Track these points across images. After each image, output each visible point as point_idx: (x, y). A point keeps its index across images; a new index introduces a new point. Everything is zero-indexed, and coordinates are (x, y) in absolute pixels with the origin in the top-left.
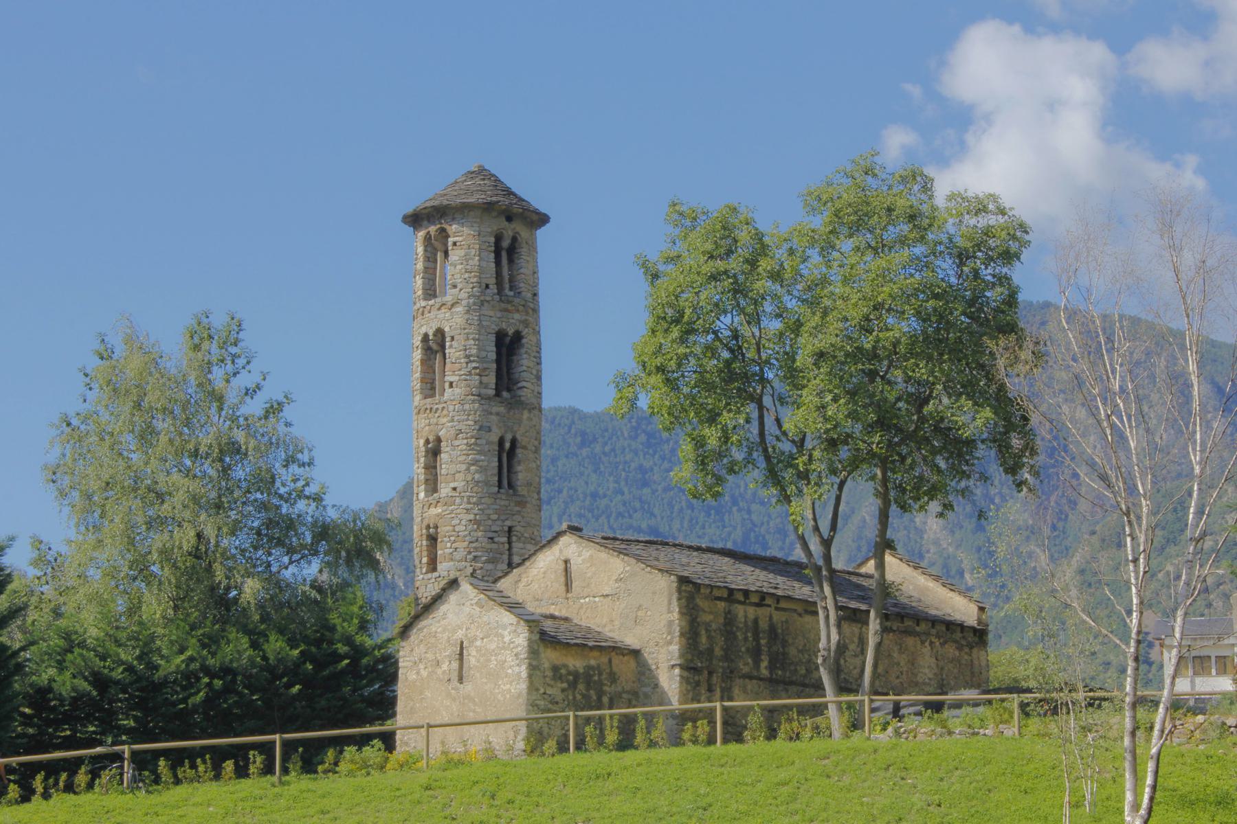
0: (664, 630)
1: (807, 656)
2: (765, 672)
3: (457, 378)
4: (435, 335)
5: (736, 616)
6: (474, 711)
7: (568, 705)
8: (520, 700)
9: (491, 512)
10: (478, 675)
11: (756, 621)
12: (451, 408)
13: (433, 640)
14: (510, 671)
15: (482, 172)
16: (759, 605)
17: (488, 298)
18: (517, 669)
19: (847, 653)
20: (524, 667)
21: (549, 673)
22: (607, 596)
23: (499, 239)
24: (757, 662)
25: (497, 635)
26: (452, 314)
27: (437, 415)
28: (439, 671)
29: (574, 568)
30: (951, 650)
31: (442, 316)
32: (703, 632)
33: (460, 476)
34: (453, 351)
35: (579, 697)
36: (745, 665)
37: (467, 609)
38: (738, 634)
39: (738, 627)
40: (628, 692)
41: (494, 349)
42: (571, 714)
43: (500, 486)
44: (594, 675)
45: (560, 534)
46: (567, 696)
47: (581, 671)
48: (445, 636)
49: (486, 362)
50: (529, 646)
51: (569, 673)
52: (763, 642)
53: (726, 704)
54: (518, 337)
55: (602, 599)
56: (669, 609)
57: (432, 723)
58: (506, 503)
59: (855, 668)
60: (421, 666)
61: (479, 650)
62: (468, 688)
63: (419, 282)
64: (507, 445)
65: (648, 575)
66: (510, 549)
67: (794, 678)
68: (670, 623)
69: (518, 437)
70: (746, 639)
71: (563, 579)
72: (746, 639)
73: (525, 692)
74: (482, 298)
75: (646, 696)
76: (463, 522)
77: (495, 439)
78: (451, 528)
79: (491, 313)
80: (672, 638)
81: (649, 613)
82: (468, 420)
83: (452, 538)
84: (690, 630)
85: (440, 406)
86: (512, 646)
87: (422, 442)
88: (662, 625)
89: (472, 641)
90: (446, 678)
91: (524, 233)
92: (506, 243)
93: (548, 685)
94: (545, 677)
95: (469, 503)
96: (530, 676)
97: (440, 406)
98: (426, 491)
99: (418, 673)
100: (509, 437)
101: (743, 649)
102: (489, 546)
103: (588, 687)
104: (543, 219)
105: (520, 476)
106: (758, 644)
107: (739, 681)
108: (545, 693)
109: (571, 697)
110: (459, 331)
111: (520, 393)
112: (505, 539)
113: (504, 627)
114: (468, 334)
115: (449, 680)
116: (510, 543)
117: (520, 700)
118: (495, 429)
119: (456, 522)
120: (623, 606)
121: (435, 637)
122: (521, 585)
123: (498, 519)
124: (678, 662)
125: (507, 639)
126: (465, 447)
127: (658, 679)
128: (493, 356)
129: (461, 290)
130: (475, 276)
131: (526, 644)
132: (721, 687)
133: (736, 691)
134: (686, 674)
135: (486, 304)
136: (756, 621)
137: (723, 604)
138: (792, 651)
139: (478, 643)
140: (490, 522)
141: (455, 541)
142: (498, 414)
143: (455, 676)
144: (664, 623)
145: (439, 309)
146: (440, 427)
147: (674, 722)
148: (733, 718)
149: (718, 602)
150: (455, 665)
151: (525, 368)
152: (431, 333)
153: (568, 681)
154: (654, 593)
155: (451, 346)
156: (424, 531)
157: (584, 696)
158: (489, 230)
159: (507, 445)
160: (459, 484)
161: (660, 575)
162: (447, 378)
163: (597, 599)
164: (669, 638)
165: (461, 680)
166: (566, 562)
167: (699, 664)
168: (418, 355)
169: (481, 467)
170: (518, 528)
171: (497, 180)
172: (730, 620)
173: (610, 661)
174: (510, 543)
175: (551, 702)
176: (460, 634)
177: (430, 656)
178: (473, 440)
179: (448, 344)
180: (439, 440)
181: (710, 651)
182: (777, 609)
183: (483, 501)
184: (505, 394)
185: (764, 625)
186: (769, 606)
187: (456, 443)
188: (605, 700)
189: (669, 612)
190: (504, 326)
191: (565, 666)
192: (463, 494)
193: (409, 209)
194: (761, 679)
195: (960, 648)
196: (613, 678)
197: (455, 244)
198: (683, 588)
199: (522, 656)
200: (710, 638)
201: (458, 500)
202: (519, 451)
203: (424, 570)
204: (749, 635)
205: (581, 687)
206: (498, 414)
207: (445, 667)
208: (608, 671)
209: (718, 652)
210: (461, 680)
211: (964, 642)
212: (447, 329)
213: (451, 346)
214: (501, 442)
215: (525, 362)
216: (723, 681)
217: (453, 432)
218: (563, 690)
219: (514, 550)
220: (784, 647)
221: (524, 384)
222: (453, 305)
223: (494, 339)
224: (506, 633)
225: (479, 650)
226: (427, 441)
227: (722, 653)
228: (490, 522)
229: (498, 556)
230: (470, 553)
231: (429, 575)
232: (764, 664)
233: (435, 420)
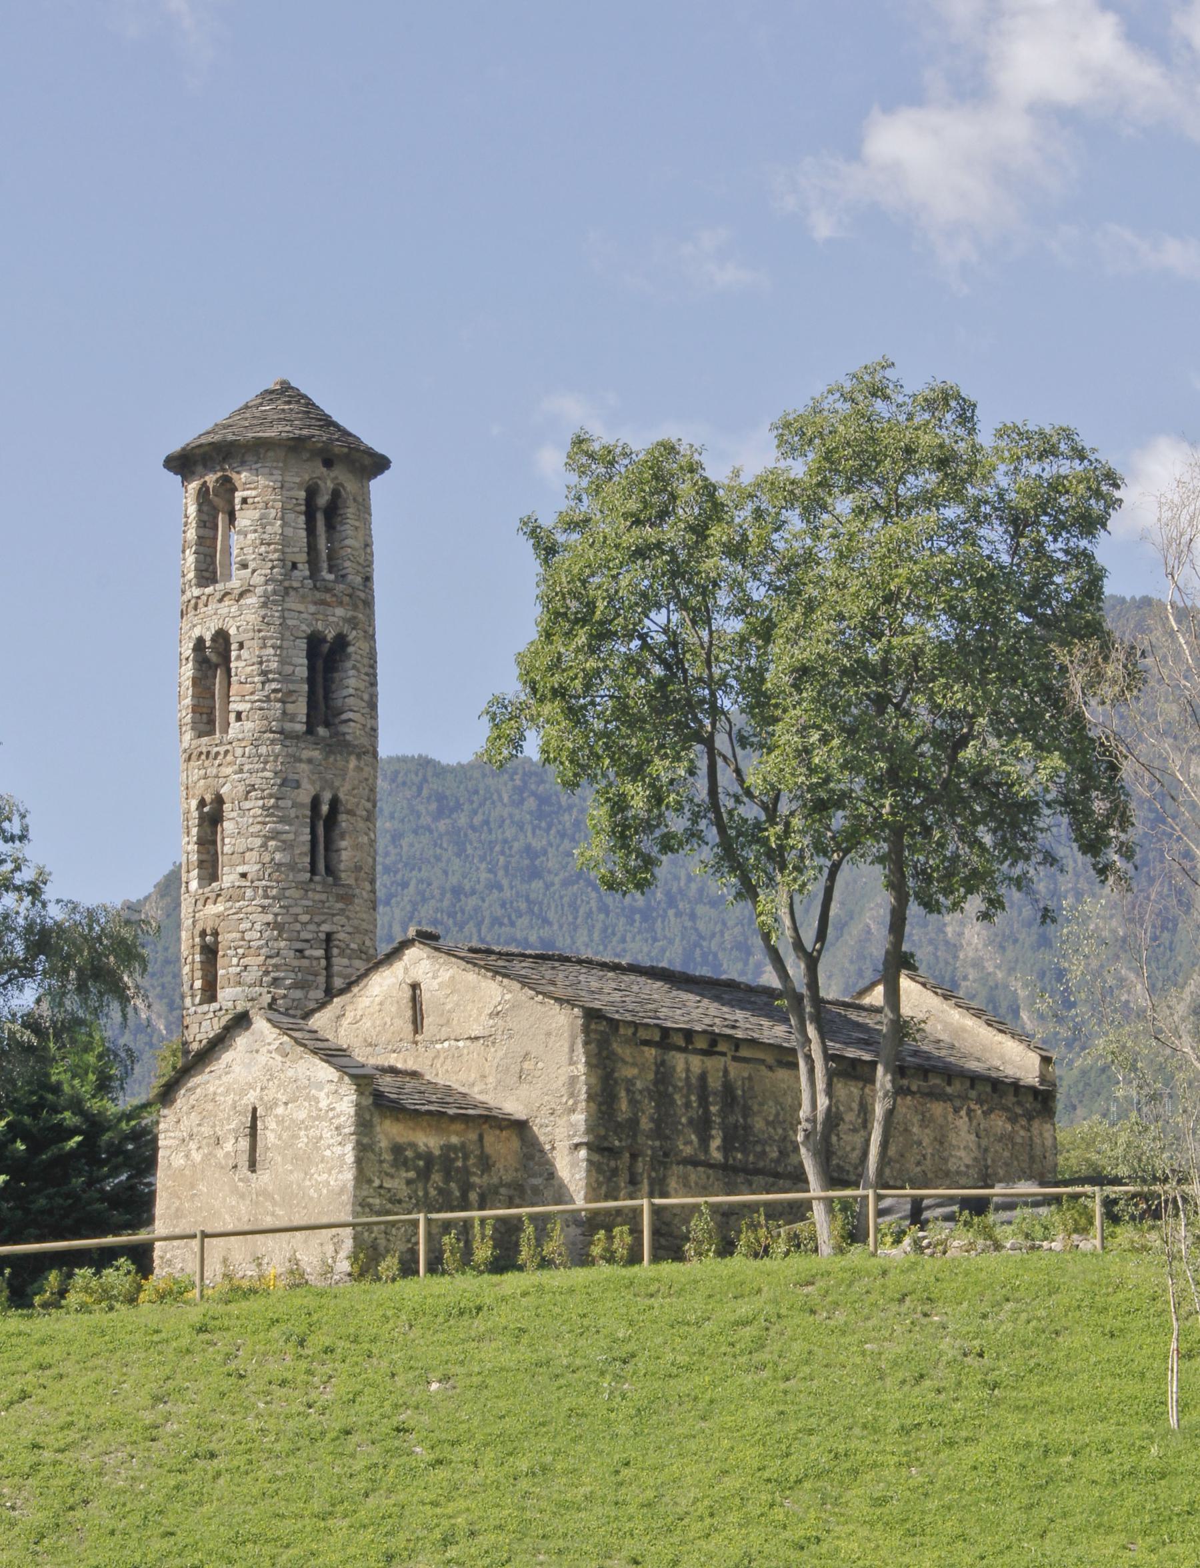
0: (563, 1091)
1: (780, 1131)
2: (717, 1155)
3: (248, 706)
4: (213, 640)
5: (674, 1068)
6: (273, 1214)
7: (417, 1205)
8: (344, 1198)
9: (299, 910)
10: (280, 1159)
11: (703, 1077)
12: (239, 752)
13: (210, 1106)
14: (328, 1153)
15: (285, 391)
16: (708, 1053)
17: (295, 584)
18: (338, 1150)
19: (843, 1127)
20: (349, 1147)
21: (388, 1157)
22: (477, 1038)
23: (312, 492)
24: (705, 1141)
25: (308, 1098)
27: (217, 762)
28: (220, 1154)
29: (426, 996)
30: (999, 1123)
31: (226, 610)
32: (623, 1094)
33: (252, 856)
34: (242, 665)
35: (433, 1192)
36: (687, 1145)
37: (262, 1059)
38: (677, 1096)
39: (675, 1087)
40: (508, 1186)
41: (305, 661)
42: (421, 1216)
43: (313, 871)
44: (457, 1159)
45: (405, 944)
46: (416, 1192)
47: (437, 1152)
48: (229, 1099)
49: (293, 682)
50: (357, 1114)
51: (419, 1156)
52: (713, 1109)
53: (657, 1201)
54: (341, 642)
55: (468, 1043)
56: (571, 1058)
57: (209, 1230)
58: (323, 897)
59: (853, 1149)
60: (193, 1145)
61: (280, 1121)
62: (263, 1178)
63: (191, 559)
64: (325, 808)
65: (539, 1007)
66: (328, 967)
67: (761, 1164)
68: (573, 1080)
69: (341, 796)
70: (688, 1105)
71: (409, 1013)
72: (688, 1105)
73: (351, 1184)
74: (286, 584)
75: (536, 1191)
76: (258, 927)
77: (307, 800)
78: (239, 935)
79: (301, 607)
80: (576, 1103)
81: (540, 1065)
82: (264, 770)
83: (240, 951)
84: (603, 1090)
85: (222, 749)
86: (331, 1114)
87: (194, 803)
88: (560, 1083)
89: (270, 1108)
90: (231, 1163)
91: (350, 486)
92: (323, 500)
93: (387, 1174)
94: (381, 1162)
95: (266, 897)
96: (359, 1161)
97: (222, 749)
98: (200, 878)
99: (187, 1156)
100: (327, 796)
101: (684, 1120)
102: (296, 963)
103: (448, 1178)
104: (380, 464)
105: (345, 855)
106: (707, 1112)
107: (677, 1170)
108: (381, 1187)
109: (421, 1194)
110: (251, 634)
111: (344, 728)
112: (320, 953)
113: (320, 1086)
114: (264, 638)
115: (235, 1167)
116: (328, 957)
117: (344, 1198)
118: (305, 784)
119: (245, 925)
120: (500, 1054)
121: (213, 1100)
122: (345, 1022)
123: (310, 922)
124: (585, 1140)
125: (323, 1104)
126: (259, 812)
127: (553, 1165)
128: (302, 672)
129: (254, 571)
130: (276, 551)
131: (352, 1111)
132: (649, 1177)
133: (673, 1184)
134: (596, 1157)
135: (292, 593)
136: (703, 1077)
137: (653, 1051)
138: (759, 1124)
139: (280, 1110)
140: (298, 927)
141: (244, 956)
142: (310, 761)
143: (244, 1160)
144: (563, 1079)
145: (221, 600)
146: (221, 780)
147: (579, 1231)
148: (667, 1224)
149: (646, 1049)
150: (244, 1144)
151: (351, 691)
152: (208, 637)
153: (416, 1168)
154: (548, 1034)
155: (239, 658)
156: (197, 940)
157: (441, 1191)
158: (297, 480)
159: (325, 808)
160: (252, 869)
161: (557, 1006)
162: (232, 706)
163: (461, 1044)
164: (571, 1102)
165: (253, 1166)
166: (415, 987)
167: (617, 1143)
168: (188, 670)
169: (284, 842)
170: (341, 936)
171: (310, 403)
172: (663, 1075)
173: (481, 1138)
174: (328, 957)
175: (390, 1201)
176: (252, 1097)
177: (206, 1130)
178: (272, 801)
179: (234, 654)
180: (219, 800)
181: (634, 1123)
183: (287, 893)
184: (322, 731)
185: (714, 1083)
186: (724, 1054)
187: (247, 805)
188: (473, 1196)
189: (572, 1063)
190: (320, 626)
191: (413, 1145)
192: (256, 883)
193: (175, 447)
195: (1013, 1119)
196: (486, 1164)
197: (244, 501)
198: (593, 1026)
199: (347, 1130)
200: (633, 1102)
201: (249, 893)
202: (342, 817)
203: (197, 1000)
204: (693, 1098)
205: (437, 1177)
206: (310, 761)
207: (229, 1146)
208: (478, 1152)
209: (645, 1124)
210: (253, 1166)
211: (1019, 1111)
212: (232, 631)
213: (239, 658)
214: (315, 803)
215: (352, 682)
216: (653, 1169)
217: (241, 788)
218: (409, 1182)
219: (336, 969)
221: (350, 715)
222: (241, 595)
223: (305, 646)
224: (322, 1095)
225: (280, 1121)
226: (202, 803)
227: (651, 1125)
228: (298, 927)
229: (311, 978)
230: (267, 973)
231: (205, 1007)
232: (716, 1143)
233: (214, 771)
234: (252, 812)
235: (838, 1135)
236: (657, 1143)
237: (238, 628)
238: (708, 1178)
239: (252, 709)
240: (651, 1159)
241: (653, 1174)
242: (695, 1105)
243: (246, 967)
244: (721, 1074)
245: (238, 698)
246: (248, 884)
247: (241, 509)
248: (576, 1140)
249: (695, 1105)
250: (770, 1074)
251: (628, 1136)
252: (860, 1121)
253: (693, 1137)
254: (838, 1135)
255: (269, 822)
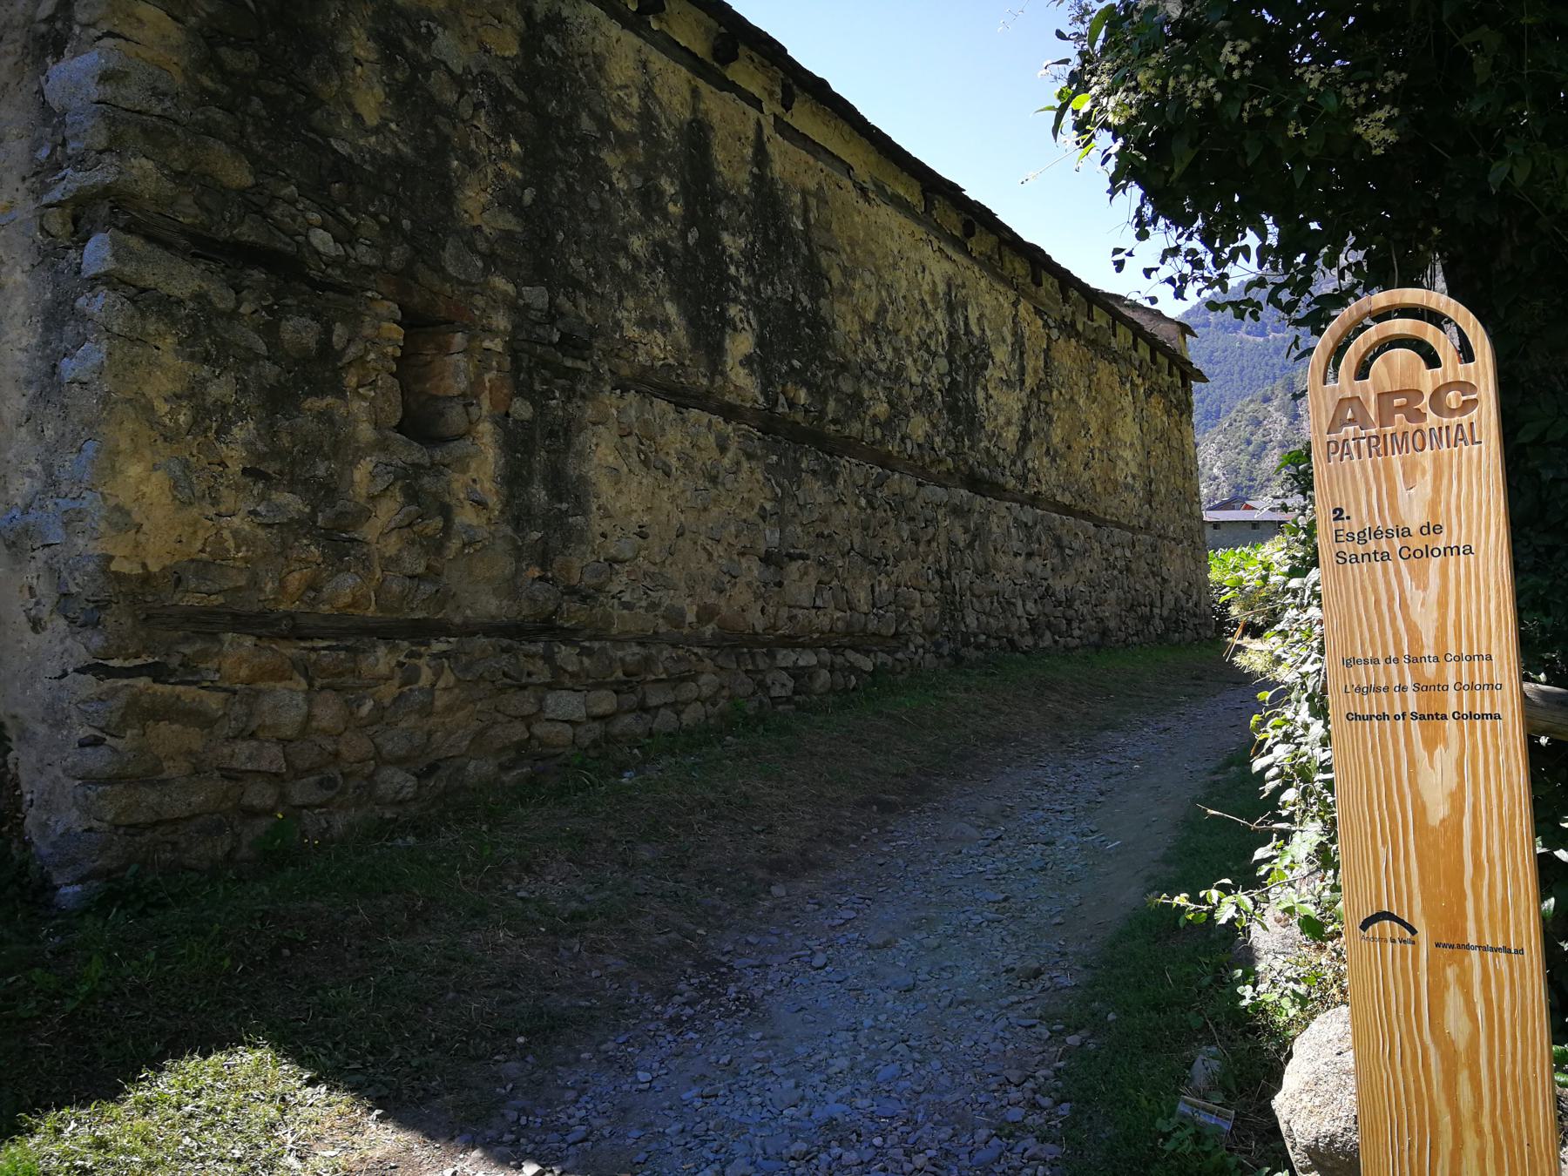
2: (743, 382)
32: (359, 44)
38: (612, 159)
52: (733, 244)
59: (1009, 423)
67: (855, 428)
70: (649, 199)
101: (636, 243)
106: (710, 241)
132: (502, 419)
136: (697, 133)
138: (846, 327)
148: (585, 597)
167: (322, 240)
182: (783, 128)
194: (730, 413)
204: (668, 187)
216: (522, 389)
220: (816, 294)
232: (741, 345)
235: (985, 388)
236: (537, 296)
238: (723, 449)
240: (513, 350)
241: (522, 409)
242: (674, 209)
244: (749, 152)
248: (73, 181)
249: (674, 209)
250: (862, 204)
251: (390, 229)
252: (1015, 366)
253: (671, 309)
254: (985, 388)
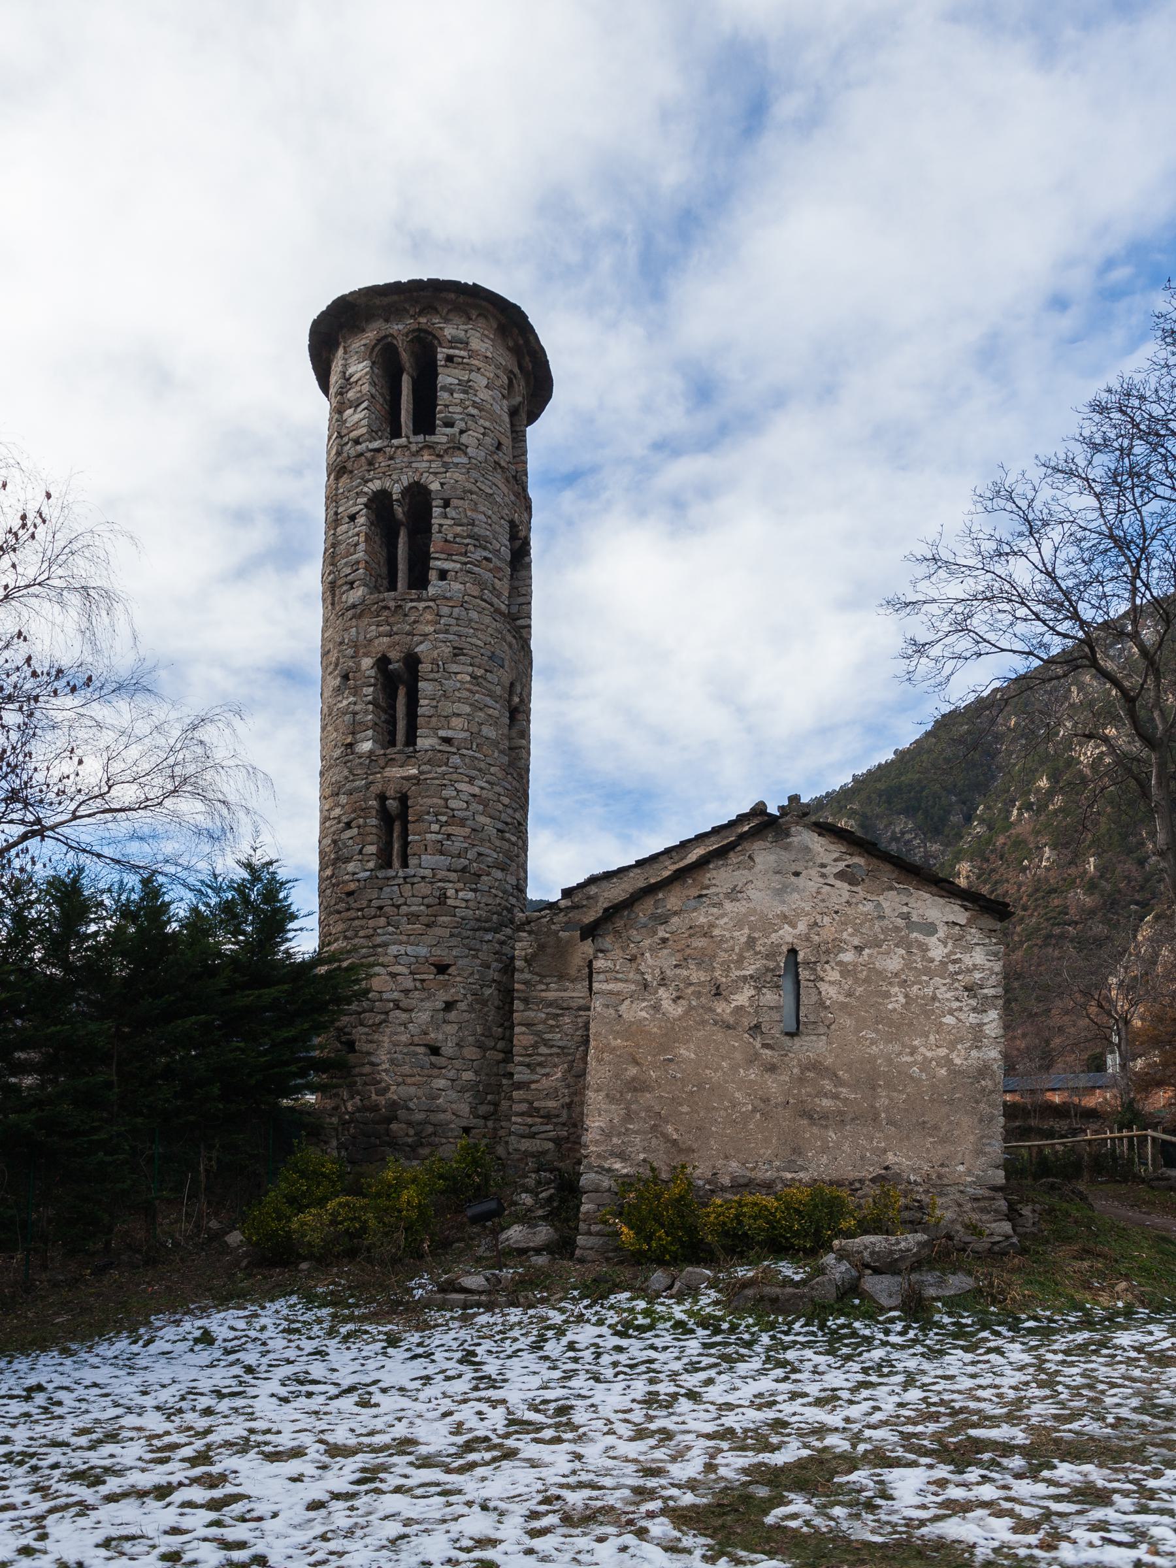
26: (446, 465)
83: (444, 819)
126: (468, 678)
141: (447, 823)
179: (436, 511)
187: (454, 668)
197: (450, 359)
212: (435, 486)
217: (447, 650)
234: (459, 677)
237: (442, 484)
239: (461, 570)
243: (449, 835)
245: (443, 556)
246: (454, 750)
247: (446, 366)
255: (477, 692)
